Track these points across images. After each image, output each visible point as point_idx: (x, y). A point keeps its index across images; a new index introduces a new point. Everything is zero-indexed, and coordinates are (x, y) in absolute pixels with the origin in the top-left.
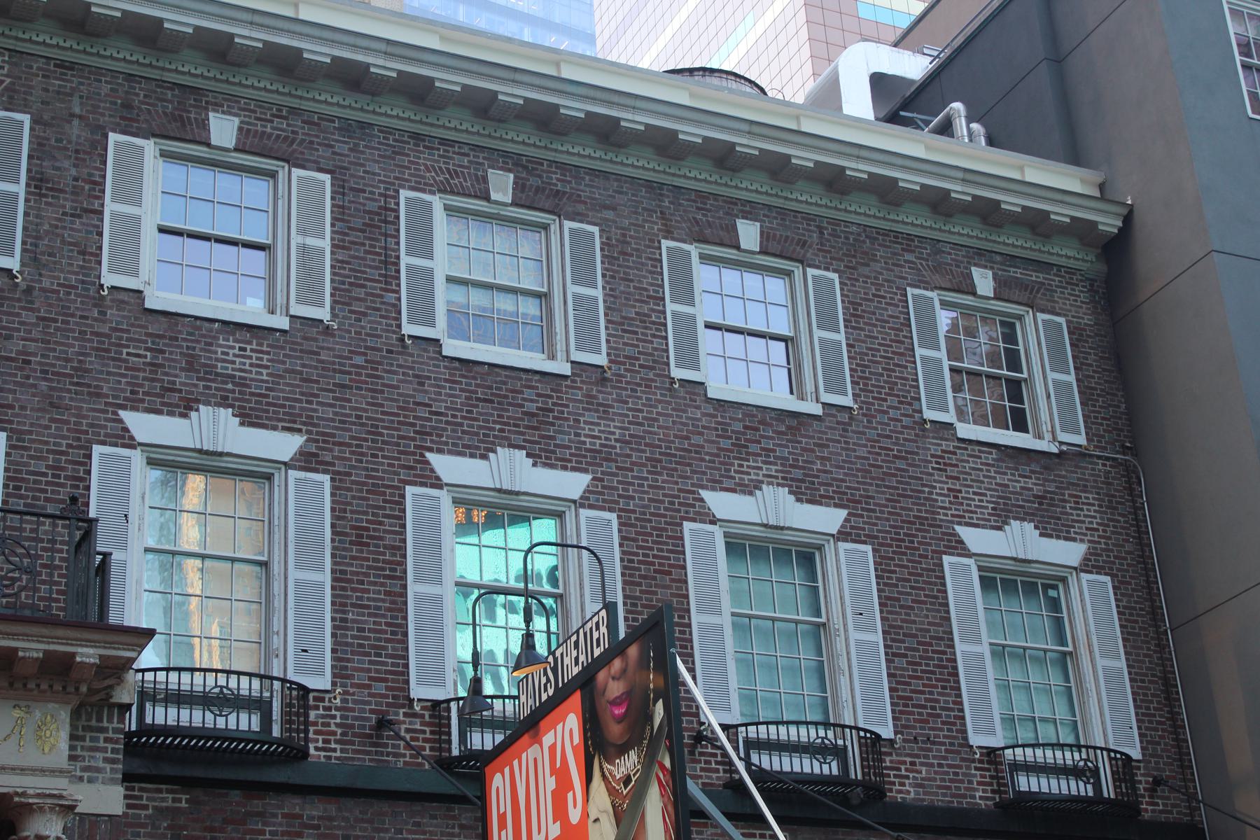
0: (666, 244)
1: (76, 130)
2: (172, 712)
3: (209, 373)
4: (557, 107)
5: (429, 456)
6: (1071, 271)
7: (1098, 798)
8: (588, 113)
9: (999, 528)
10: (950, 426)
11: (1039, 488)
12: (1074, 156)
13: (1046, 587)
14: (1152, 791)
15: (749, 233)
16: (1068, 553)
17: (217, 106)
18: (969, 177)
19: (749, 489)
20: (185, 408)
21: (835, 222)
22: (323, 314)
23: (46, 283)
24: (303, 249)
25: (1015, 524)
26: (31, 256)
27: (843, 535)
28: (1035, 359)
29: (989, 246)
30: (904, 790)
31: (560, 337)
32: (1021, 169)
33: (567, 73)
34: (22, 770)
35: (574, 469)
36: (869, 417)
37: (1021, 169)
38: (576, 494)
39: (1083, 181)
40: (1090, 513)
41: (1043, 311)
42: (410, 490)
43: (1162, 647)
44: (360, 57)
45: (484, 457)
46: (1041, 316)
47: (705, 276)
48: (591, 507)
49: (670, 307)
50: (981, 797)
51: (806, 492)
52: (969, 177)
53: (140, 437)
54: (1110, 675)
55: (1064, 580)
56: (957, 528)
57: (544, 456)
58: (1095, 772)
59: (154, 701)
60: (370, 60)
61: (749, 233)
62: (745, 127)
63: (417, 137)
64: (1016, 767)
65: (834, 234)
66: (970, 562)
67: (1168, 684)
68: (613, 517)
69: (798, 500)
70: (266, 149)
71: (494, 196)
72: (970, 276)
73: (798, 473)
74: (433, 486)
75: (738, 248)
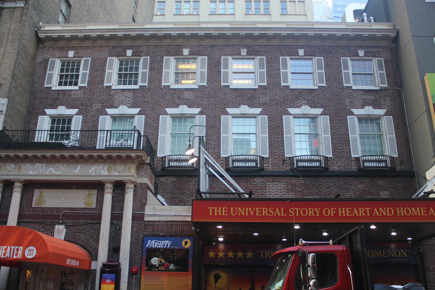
0: (281, 57)
1: (158, 58)
2: (175, 163)
3: (182, 98)
4: (253, 33)
5: (227, 109)
6: (385, 47)
7: (386, 167)
8: (260, 34)
9: (363, 108)
10: (351, 87)
11: (373, 98)
12: (388, 19)
13: (376, 120)
14: (401, 164)
15: (301, 52)
16: (381, 112)
17: (185, 48)
18: (354, 30)
19: (299, 107)
20: (177, 106)
21: (323, 46)
22: (205, 84)
23: (152, 87)
24: (201, 72)
25: (367, 107)
26: (150, 83)
27: (322, 114)
28: (375, 69)
29: (363, 45)
30: (335, 168)
31: (257, 81)
32: (371, 26)
33: (258, 26)
34: (125, 176)
35: (258, 108)
36: (330, 87)
37: (371, 26)
38: (258, 113)
39: (388, 26)
40: (388, 102)
41: (377, 57)
42: (222, 116)
43: (406, 131)
44: (210, 32)
45: (238, 108)
46: (376, 59)
47: (290, 63)
48: (262, 115)
49: (281, 71)
50: (354, 168)
51: (313, 105)
52: (354, 30)
53: (169, 113)
54: (391, 139)
55: (380, 118)
56: (352, 109)
57: (251, 106)
58: (386, 161)
59: (172, 161)
60: (212, 32)
61: (301, 52)
62: (297, 29)
63: (226, 45)
64: (364, 161)
65: (323, 49)
66: (355, 117)
67: (407, 139)
68: (267, 116)
69: (311, 108)
70: (194, 54)
71: (242, 54)
72: (358, 52)
73: (311, 102)
74: (227, 115)
75: (299, 55)
